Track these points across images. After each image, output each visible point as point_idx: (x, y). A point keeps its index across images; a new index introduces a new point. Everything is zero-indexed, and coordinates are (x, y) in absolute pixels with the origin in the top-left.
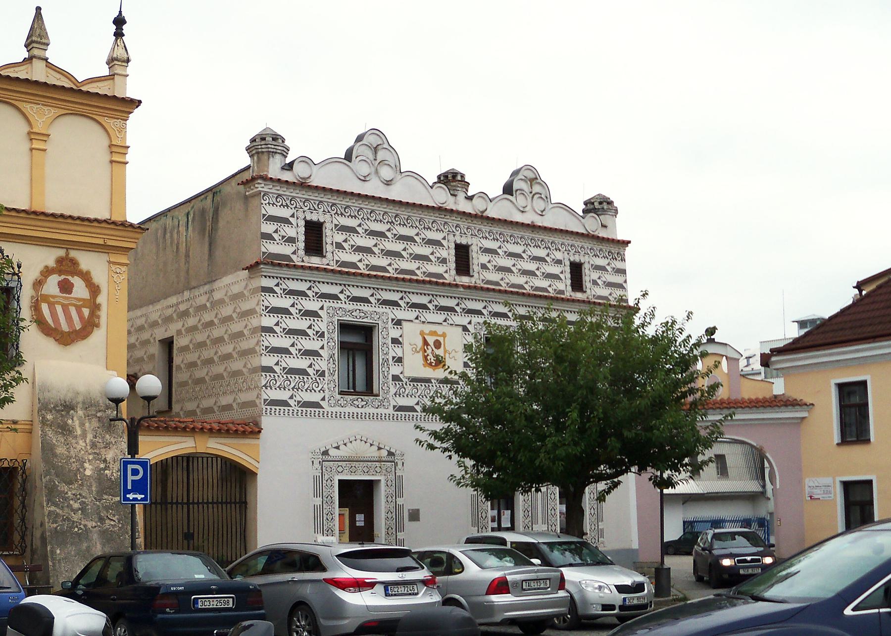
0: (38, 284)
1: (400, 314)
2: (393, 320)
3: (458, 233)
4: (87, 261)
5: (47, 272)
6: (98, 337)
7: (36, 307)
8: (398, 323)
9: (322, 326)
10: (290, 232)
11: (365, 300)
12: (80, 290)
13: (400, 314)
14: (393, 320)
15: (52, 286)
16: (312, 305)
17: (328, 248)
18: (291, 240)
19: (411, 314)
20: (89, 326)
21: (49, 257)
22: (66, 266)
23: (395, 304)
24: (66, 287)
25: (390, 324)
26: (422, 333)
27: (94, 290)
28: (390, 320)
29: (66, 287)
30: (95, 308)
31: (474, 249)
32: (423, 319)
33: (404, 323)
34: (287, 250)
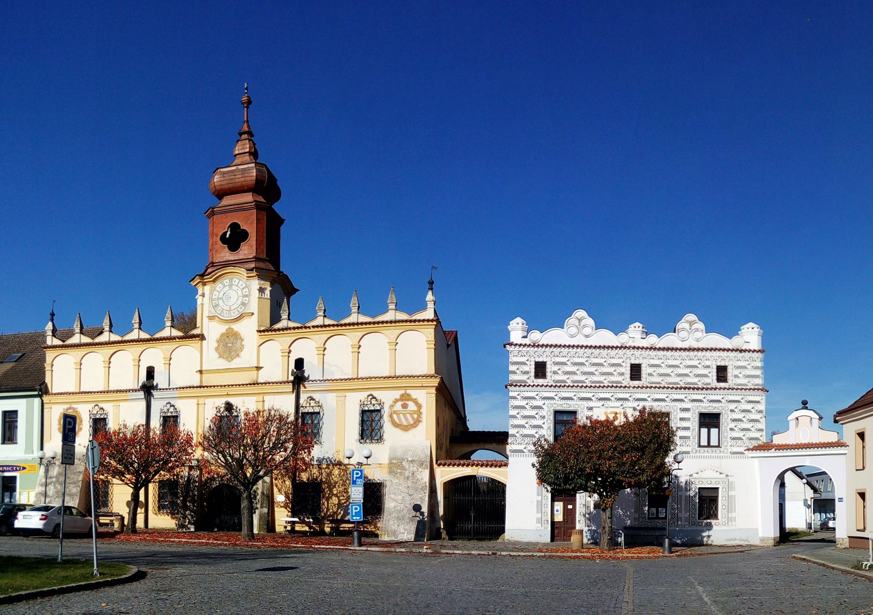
0: (392, 406)
4: (414, 394)
5: (396, 401)
6: (422, 426)
7: (391, 416)
9: (543, 413)
10: (526, 368)
12: (412, 406)
15: (398, 407)
16: (539, 403)
17: (548, 374)
18: (527, 373)
20: (417, 422)
21: (397, 394)
22: (405, 397)
24: (405, 406)
27: (419, 406)
29: (405, 406)
30: (420, 414)
34: (524, 377)
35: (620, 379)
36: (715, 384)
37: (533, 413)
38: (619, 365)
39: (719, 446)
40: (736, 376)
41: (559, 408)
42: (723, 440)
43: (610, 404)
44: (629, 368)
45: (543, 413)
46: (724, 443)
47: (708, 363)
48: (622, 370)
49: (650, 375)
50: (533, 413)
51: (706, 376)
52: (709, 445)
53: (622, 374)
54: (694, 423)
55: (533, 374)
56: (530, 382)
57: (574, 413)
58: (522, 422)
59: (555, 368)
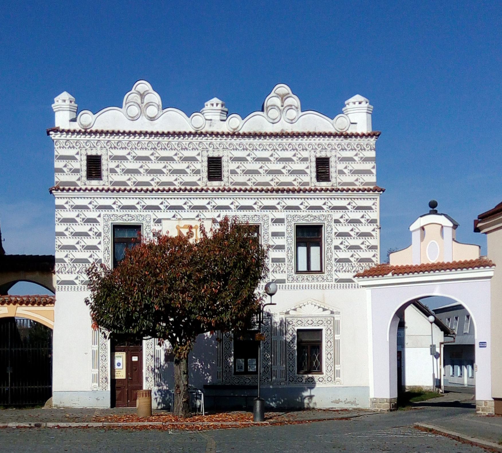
1: (159, 215)
2: (154, 220)
3: (221, 149)
8: (159, 221)
9: (99, 228)
11: (133, 208)
13: (159, 215)
14: (154, 220)
17: (104, 173)
19: (170, 214)
23: (157, 208)
25: (152, 223)
26: (178, 227)
28: (152, 220)
31: (224, 160)
32: (179, 217)
33: (163, 221)
34: (73, 178)
35: (194, 178)
36: (314, 184)
37: (85, 228)
38: (193, 159)
39: (321, 272)
40: (341, 172)
41: (119, 222)
42: (325, 262)
43: (184, 214)
44: (206, 164)
45: (99, 228)
46: (327, 268)
47: (305, 154)
48: (197, 166)
49: (233, 172)
50: (85, 228)
51: (302, 172)
52: (309, 271)
53: (197, 172)
54: (289, 240)
55: (84, 173)
56: (80, 185)
57: (138, 228)
58: (72, 242)
59: (113, 165)
